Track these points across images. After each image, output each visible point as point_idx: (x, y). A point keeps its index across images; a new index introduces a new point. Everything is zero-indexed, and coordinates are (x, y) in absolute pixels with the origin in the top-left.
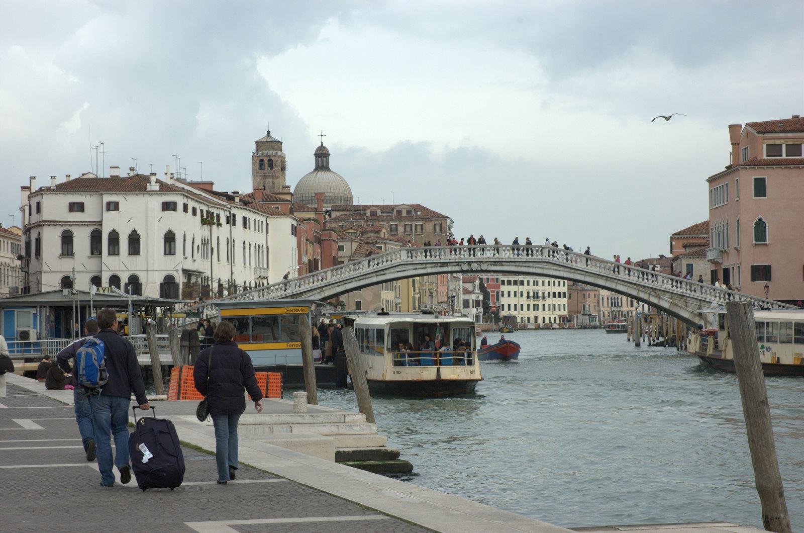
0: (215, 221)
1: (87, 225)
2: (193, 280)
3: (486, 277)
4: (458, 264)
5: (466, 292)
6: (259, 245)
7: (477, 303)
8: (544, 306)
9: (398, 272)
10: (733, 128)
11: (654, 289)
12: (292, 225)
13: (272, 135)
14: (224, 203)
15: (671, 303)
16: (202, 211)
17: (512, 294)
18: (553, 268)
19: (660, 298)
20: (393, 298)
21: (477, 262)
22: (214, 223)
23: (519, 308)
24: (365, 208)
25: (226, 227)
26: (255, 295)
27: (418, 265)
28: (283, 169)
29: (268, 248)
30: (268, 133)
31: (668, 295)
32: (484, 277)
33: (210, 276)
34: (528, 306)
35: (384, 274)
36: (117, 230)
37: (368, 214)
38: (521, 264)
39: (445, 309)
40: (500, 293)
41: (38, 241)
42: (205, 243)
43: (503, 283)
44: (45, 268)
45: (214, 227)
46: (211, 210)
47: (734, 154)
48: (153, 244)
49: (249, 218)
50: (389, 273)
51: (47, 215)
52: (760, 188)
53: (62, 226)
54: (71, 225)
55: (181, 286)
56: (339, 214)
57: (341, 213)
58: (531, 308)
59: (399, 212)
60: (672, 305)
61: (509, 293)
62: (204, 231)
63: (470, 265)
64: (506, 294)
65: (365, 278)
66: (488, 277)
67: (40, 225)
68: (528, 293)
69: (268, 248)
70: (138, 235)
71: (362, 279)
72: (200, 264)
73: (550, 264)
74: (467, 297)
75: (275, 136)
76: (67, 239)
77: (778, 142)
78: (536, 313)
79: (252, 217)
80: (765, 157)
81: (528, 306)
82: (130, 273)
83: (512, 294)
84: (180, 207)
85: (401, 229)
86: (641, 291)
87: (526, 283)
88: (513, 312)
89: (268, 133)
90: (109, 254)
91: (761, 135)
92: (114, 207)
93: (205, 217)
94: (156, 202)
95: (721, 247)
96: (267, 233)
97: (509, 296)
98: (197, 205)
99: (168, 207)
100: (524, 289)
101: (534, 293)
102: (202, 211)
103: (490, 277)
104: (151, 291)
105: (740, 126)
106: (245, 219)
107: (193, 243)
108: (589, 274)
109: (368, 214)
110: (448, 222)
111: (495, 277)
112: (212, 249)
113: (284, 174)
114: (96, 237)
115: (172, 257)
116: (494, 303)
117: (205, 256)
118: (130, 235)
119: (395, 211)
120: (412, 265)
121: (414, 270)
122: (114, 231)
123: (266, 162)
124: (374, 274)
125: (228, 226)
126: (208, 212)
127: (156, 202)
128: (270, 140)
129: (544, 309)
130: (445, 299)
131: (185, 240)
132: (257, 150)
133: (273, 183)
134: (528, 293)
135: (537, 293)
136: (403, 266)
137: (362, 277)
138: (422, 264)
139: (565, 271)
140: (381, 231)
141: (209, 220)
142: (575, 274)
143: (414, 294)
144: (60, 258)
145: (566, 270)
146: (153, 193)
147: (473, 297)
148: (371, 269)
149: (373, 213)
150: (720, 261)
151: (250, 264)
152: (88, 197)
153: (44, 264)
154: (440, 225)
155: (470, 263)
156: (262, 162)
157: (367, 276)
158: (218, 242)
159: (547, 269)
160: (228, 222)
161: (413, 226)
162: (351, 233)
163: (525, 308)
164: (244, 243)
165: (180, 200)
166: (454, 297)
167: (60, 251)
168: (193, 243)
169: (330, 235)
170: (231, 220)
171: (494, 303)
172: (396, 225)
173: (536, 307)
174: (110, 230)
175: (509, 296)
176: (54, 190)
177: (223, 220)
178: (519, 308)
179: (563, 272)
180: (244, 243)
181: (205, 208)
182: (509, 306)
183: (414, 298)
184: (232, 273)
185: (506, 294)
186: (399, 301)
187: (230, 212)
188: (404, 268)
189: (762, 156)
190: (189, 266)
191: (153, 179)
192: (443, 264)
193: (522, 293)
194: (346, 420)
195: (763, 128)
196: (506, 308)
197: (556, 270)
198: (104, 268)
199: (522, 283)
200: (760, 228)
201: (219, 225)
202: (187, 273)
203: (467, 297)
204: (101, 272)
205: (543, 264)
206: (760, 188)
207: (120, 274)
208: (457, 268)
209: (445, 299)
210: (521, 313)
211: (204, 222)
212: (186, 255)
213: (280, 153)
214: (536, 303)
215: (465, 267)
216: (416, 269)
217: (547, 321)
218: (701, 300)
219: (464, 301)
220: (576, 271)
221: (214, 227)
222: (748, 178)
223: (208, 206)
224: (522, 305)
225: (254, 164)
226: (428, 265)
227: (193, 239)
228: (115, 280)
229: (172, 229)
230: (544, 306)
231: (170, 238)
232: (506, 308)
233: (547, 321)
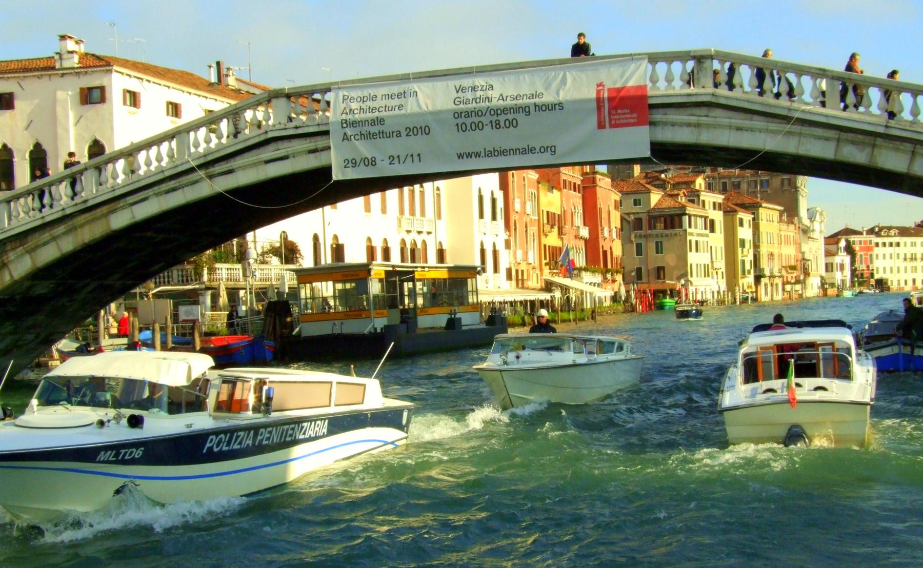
3: (858, 239)
9: (267, 162)
17: (888, 256)
18: (726, 121)
23: (895, 270)
27: (319, 138)
32: (856, 239)
34: (906, 268)
35: (230, 172)
36: (10, 146)
40: (874, 257)
43: (877, 245)
50: (244, 167)
58: (909, 270)
61: (884, 255)
64: (881, 257)
65: (182, 187)
66: (860, 239)
68: (905, 255)
71: (174, 190)
73: (718, 112)
74: (830, 260)
78: (914, 276)
81: (906, 268)
83: (888, 256)
87: (902, 244)
100: (901, 250)
101: (912, 254)
103: (862, 239)
108: (851, 136)
111: (868, 239)
116: (868, 267)
121: (312, 155)
124: (201, 173)
134: (905, 255)
135: (916, 254)
137: (172, 184)
139: (767, 131)
140: (694, 182)
142: (803, 140)
143: (742, 257)
154: (789, 179)
157: (184, 180)
159: (708, 126)
161: (758, 181)
162: (658, 185)
163: (902, 270)
171: (868, 267)
172: (739, 182)
178: (895, 270)
179: (763, 135)
185: (881, 257)
188: (284, 148)
193: (898, 255)
197: (739, 129)
199: (898, 245)
205: (703, 111)
219: (827, 265)
220: (806, 130)
224: (898, 268)
232: (881, 271)
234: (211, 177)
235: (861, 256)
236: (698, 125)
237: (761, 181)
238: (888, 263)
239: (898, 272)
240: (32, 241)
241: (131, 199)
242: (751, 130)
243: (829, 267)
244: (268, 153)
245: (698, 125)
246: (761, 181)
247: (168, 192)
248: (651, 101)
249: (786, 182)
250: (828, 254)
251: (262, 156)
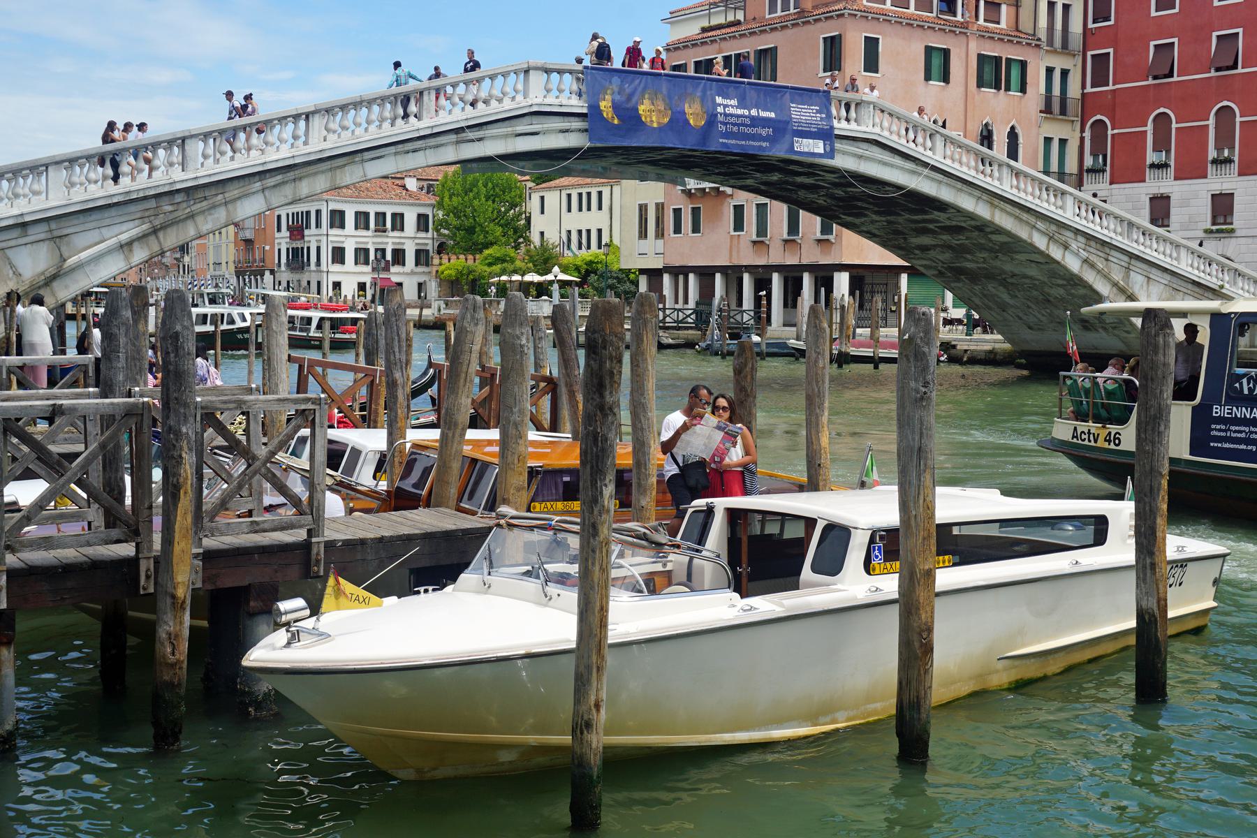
15: (1086, 261)
19: (1066, 247)
35: (480, 140)
60: (1085, 266)
86: (1038, 230)
120: (561, 119)
121: (561, 135)
124: (453, 137)
136: (535, 119)
139: (902, 169)
145: (909, 165)
157: (432, 142)
205: (865, 145)
216: (567, 131)
234: (458, 142)
236: (860, 157)
240: (233, 192)
241: (367, 155)
242: (892, 166)
244: (521, 127)
245: (860, 157)
247: (408, 152)
248: (836, 132)
251: (518, 128)
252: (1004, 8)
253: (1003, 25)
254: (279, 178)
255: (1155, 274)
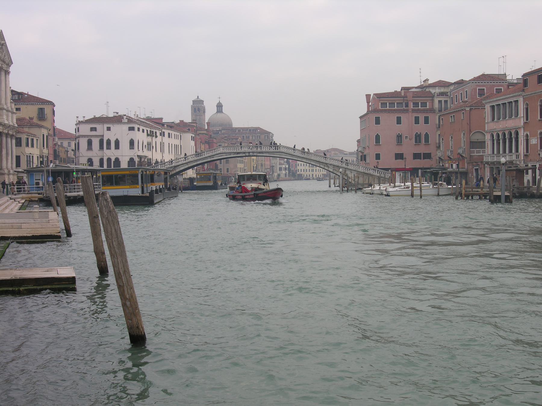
0: (154, 135)
1: (98, 137)
2: (143, 160)
4: (244, 153)
5: (280, 164)
6: (176, 145)
7: (285, 169)
8: (316, 170)
10: (368, 96)
11: (326, 164)
12: (192, 136)
13: (199, 98)
14: (160, 127)
16: (147, 131)
19: (329, 167)
20: (243, 167)
21: (252, 152)
22: (153, 136)
23: (305, 171)
24: (236, 128)
25: (159, 137)
26: (159, 166)
28: (204, 112)
29: (181, 146)
30: (198, 96)
31: (332, 166)
33: (152, 158)
34: (309, 170)
36: (110, 139)
37: (237, 131)
38: (271, 153)
39: (269, 171)
41: (78, 143)
42: (149, 144)
44: (81, 155)
45: (154, 138)
46: (152, 130)
47: (369, 106)
48: (125, 145)
49: (171, 134)
51: (81, 133)
52: (378, 121)
53: (87, 137)
54: (91, 137)
55: (137, 162)
56: (225, 131)
57: (226, 131)
59: (250, 130)
62: (149, 139)
63: (249, 154)
67: (79, 137)
69: (181, 146)
70: (119, 141)
72: (147, 153)
74: (281, 166)
75: (201, 98)
76: (90, 143)
77: (385, 102)
78: (312, 173)
79: (173, 133)
80: (380, 108)
81: (309, 170)
82: (115, 157)
84: (136, 129)
85: (251, 138)
88: (301, 173)
89: (198, 96)
90: (107, 149)
91: (379, 99)
92: (109, 129)
93: (149, 133)
94: (126, 127)
95: (364, 146)
96: (181, 139)
97: (301, 166)
98: (145, 128)
99: (131, 129)
102: (147, 131)
104: (124, 165)
105: (370, 95)
106: (169, 134)
107: (143, 144)
109: (237, 131)
110: (271, 134)
112: (153, 147)
113: (205, 114)
114: (101, 142)
115: (133, 150)
116: (295, 169)
117: (149, 149)
118: (115, 141)
119: (248, 130)
122: (109, 139)
123: (197, 109)
125: (161, 137)
126: (150, 131)
127: (126, 127)
128: (198, 100)
129: (316, 171)
130: (269, 167)
131: (138, 143)
132: (193, 104)
133: (200, 118)
138: (229, 153)
140: (238, 139)
141: (151, 134)
144: (87, 151)
145: (290, 155)
146: (125, 123)
147: (284, 166)
148: (208, 155)
149: (239, 131)
150: (363, 151)
151: (172, 153)
152: (98, 125)
153: (80, 153)
154: (268, 136)
155: (249, 153)
156: (195, 109)
158: (156, 144)
160: (161, 135)
161: (256, 136)
163: (308, 170)
164: (169, 144)
165: (136, 126)
166: (274, 166)
167: (87, 148)
168: (143, 144)
169: (213, 140)
170: (162, 134)
171: (295, 169)
173: (313, 170)
174: (107, 139)
175: (301, 166)
176: (84, 122)
177: (158, 134)
178: (305, 171)
180: (169, 144)
181: (149, 130)
182: (301, 170)
183: (254, 167)
184: (163, 157)
185: (300, 165)
186: (246, 168)
187: (162, 131)
189: (379, 107)
190: (140, 153)
191: (125, 117)
192: (238, 153)
194: (50, 222)
195: (379, 96)
196: (300, 171)
198: (105, 155)
200: (378, 138)
201: (156, 137)
202: (140, 157)
203: (281, 166)
204: (103, 156)
206: (378, 121)
207: (111, 157)
208: (244, 155)
209: (269, 167)
210: (306, 173)
211: (148, 135)
212: (139, 149)
213: (202, 105)
214: (313, 169)
215: (247, 154)
217: (317, 176)
218: (346, 168)
219: (279, 168)
221: (154, 138)
222: (373, 117)
223: (151, 128)
224: (307, 170)
225: (191, 110)
226: (232, 154)
227: (143, 142)
228: (109, 160)
229: (133, 138)
230: (316, 170)
231: (132, 143)
232: (300, 171)
233: (317, 176)
235: (292, 164)
237: (257, 136)
238: (303, 168)
239: (307, 171)
243: (280, 169)
246: (257, 136)
249: (266, 137)
250: (280, 164)
252: (428, 103)
253: (428, 107)
254: (186, 164)
255: (352, 171)
